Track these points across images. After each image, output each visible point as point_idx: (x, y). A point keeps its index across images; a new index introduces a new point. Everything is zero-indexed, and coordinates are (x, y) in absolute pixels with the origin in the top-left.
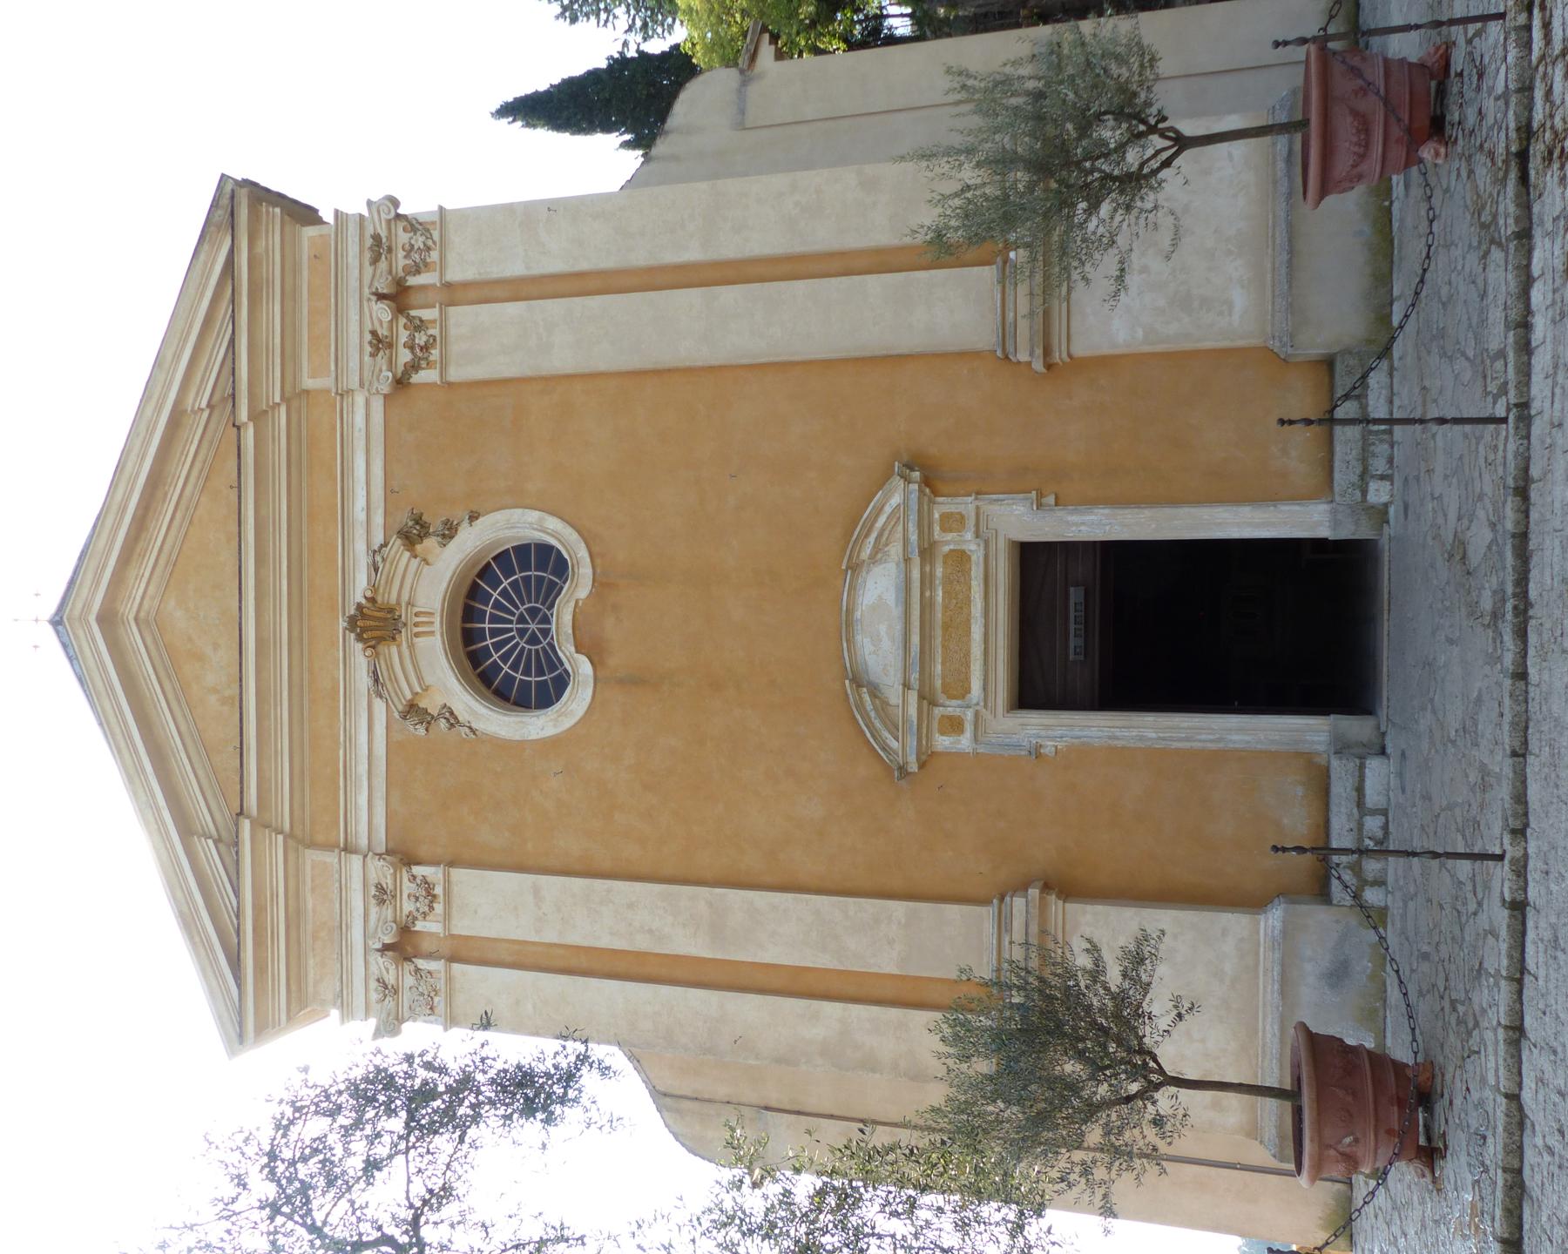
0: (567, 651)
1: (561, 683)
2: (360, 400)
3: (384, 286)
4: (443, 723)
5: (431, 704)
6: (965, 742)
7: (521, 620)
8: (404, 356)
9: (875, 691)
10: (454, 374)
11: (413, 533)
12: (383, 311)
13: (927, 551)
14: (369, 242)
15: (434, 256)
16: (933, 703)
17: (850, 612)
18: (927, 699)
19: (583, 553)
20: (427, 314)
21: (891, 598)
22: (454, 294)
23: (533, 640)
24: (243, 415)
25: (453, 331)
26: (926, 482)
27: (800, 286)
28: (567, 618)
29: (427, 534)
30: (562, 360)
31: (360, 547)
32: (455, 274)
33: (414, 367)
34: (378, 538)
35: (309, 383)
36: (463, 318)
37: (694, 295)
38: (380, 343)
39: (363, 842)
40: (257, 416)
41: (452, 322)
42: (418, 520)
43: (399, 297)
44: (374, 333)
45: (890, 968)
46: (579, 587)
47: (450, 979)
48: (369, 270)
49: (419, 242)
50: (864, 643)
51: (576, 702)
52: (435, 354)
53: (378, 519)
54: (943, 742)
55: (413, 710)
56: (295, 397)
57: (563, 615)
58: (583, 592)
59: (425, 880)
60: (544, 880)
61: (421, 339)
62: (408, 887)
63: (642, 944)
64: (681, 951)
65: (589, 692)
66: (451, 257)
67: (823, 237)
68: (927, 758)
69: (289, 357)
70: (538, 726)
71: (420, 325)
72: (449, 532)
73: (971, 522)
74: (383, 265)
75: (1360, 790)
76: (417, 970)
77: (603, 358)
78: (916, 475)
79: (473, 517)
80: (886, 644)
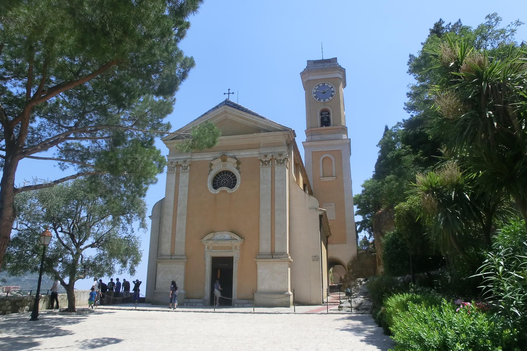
0: (220, 189)
1: (215, 187)
5: (213, 167)
7: (226, 180)
8: (264, 160)
11: (238, 163)
19: (234, 191)
20: (270, 164)
23: (223, 183)
27: (270, 224)
28: (224, 189)
29: (238, 165)
30: (262, 186)
33: (262, 162)
34: (237, 157)
36: (269, 169)
37: (270, 207)
39: (193, 157)
44: (267, 155)
47: (173, 173)
49: (281, 161)
53: (240, 157)
55: (212, 165)
57: (225, 188)
59: (187, 168)
60: (187, 187)
61: (266, 163)
62: (186, 165)
63: (179, 203)
64: (178, 209)
65: (214, 193)
70: (209, 185)
71: (269, 162)
72: (238, 168)
75: (199, 303)
76: (174, 167)
79: (240, 173)
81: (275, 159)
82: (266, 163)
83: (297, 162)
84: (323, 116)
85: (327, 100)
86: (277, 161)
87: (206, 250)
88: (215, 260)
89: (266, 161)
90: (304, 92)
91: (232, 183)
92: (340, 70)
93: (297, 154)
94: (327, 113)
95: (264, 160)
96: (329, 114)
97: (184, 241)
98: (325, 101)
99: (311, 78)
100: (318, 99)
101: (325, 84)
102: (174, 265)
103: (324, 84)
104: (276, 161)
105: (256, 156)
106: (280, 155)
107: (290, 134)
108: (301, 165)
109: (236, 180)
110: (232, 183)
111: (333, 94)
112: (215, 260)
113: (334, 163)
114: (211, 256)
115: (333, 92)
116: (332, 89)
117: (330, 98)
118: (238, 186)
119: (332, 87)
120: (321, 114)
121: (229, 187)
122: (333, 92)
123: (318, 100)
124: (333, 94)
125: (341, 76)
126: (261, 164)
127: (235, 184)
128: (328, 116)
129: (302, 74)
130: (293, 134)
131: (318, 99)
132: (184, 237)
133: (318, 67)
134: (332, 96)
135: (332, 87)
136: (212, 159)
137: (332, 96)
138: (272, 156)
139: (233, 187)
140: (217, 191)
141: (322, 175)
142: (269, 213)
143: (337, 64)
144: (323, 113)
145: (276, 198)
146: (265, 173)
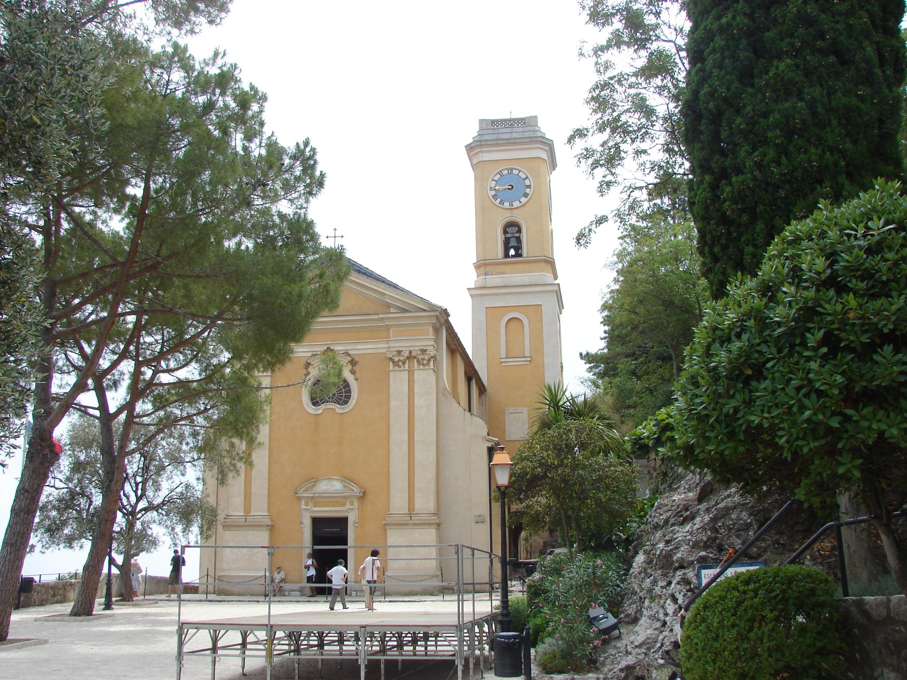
0: (323, 406)
1: (315, 403)
2: (386, 346)
3: (414, 354)
4: (305, 372)
5: (310, 369)
6: (303, 507)
8: (396, 359)
9: (314, 486)
10: (391, 373)
11: (353, 363)
12: (406, 354)
13: (346, 497)
14: (425, 348)
15: (421, 367)
16: (312, 499)
17: (333, 479)
18: (312, 498)
19: (346, 410)
20: (407, 365)
21: (336, 488)
22: (411, 372)
24: (381, 316)
25: (402, 373)
26: (361, 497)
30: (393, 403)
31: (349, 347)
32: (416, 373)
33: (394, 362)
34: (351, 352)
35: (391, 331)
36: (405, 375)
37: (406, 439)
38: (399, 352)
40: (381, 319)
41: (404, 372)
42: (356, 364)
43: (410, 357)
45: (253, 490)
46: (338, 409)
48: (418, 348)
49: (425, 362)
50: (324, 483)
51: (311, 409)
52: (397, 368)
53: (356, 352)
54: (303, 502)
55: (309, 364)
56: (388, 328)
57: (331, 406)
58: (338, 411)
61: (400, 364)
66: (420, 371)
67: (418, 471)
68: (300, 499)
69: (398, 326)
71: (404, 363)
73: (352, 507)
74: (419, 352)
75: (294, 591)
77: (393, 414)
78: (361, 495)
79: (356, 379)
80: (325, 487)
81: (415, 357)
82: (400, 364)
83: (454, 347)
84: (508, 235)
85: (516, 204)
86: (418, 361)
87: (303, 507)
88: (317, 522)
89: (399, 361)
91: (343, 395)
92: (542, 142)
93: (452, 336)
94: (517, 229)
95: (396, 359)
96: (519, 231)
97: (266, 492)
99: (486, 157)
100: (499, 200)
101: (515, 172)
102: (252, 532)
103: (512, 169)
104: (415, 360)
105: (384, 351)
106: (424, 351)
107: (441, 319)
108: (461, 351)
109: (349, 391)
110: (343, 395)
111: (528, 191)
112: (317, 522)
114: (311, 517)
115: (529, 187)
116: (527, 182)
117: (524, 200)
118: (353, 401)
119: (527, 178)
120: (505, 232)
121: (339, 403)
122: (529, 187)
123: (500, 203)
124: (528, 191)
125: (544, 155)
126: (391, 364)
127: (349, 397)
128: (517, 235)
129: (470, 148)
130: (445, 315)
131: (499, 200)
132: (266, 485)
133: (500, 136)
134: (526, 195)
135: (527, 178)
136: (310, 354)
137: (526, 195)
138: (410, 352)
139: (346, 402)
140: (320, 410)
142: (406, 448)
143: (537, 129)
144: (508, 229)
145: (417, 424)
146: (398, 381)
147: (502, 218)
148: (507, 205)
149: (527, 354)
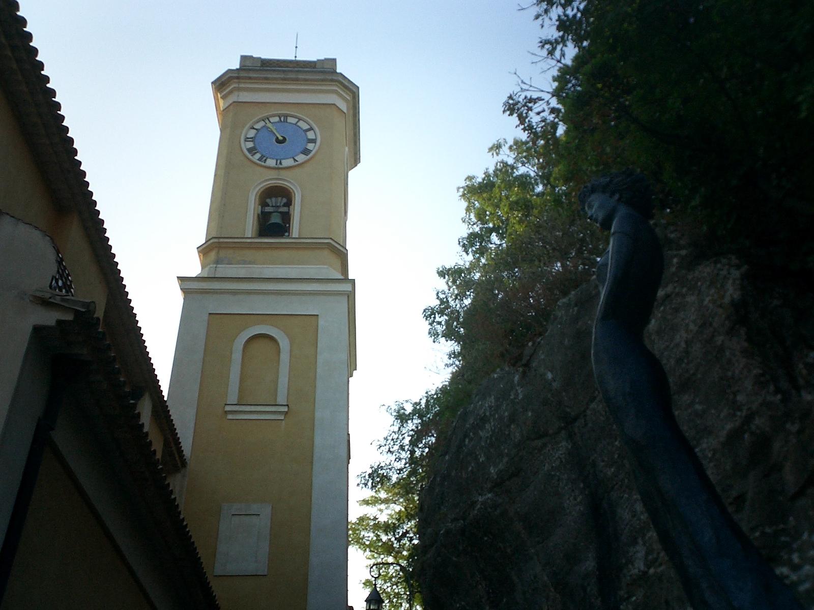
84: (267, 209)
90: (219, 132)
98: (281, 163)
101: (290, 120)
111: (310, 146)
113: (285, 357)
116: (311, 135)
117: (301, 158)
120: (264, 204)
123: (260, 159)
124: (310, 146)
128: (285, 209)
134: (306, 152)
137: (306, 152)
141: (233, 397)
144: (268, 201)
147: (261, 180)
148: (271, 162)
149: (281, 399)
